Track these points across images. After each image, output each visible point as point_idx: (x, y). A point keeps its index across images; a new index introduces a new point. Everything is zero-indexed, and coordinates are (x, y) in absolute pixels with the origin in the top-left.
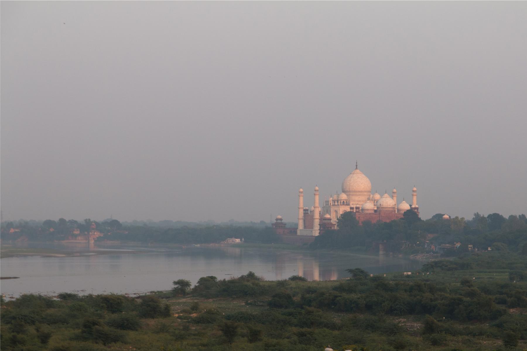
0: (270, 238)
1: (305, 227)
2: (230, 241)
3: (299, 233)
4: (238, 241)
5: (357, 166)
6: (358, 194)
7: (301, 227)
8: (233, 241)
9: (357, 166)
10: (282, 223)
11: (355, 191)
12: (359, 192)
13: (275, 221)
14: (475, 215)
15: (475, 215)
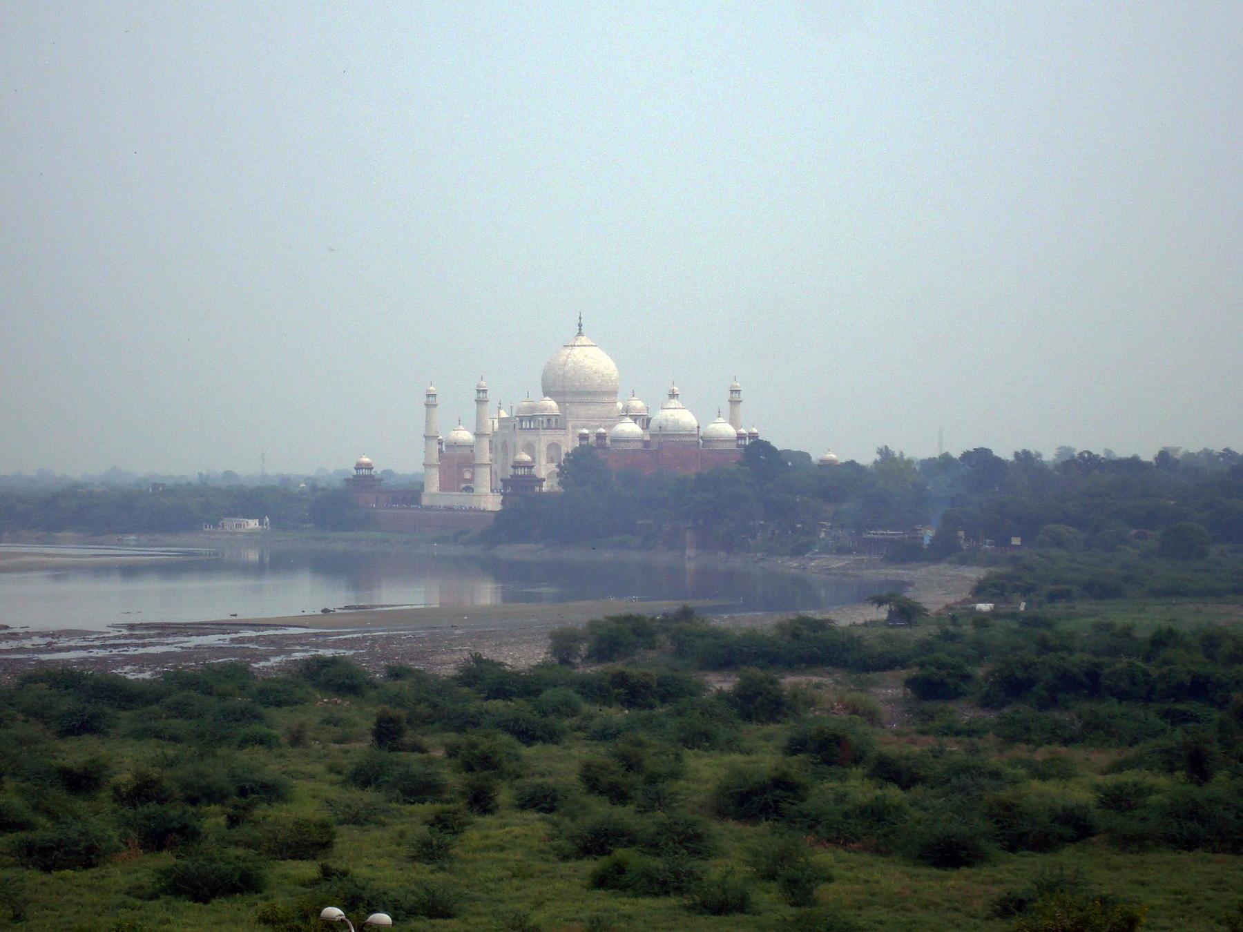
0: (339, 518)
1: (444, 486)
2: (230, 524)
3: (426, 501)
4: (253, 524)
5: (580, 325)
6: (586, 399)
7: (433, 485)
8: (239, 526)
9: (580, 325)
10: (371, 476)
11: (578, 393)
12: (590, 393)
13: (355, 472)
14: (880, 452)
15: (880, 452)
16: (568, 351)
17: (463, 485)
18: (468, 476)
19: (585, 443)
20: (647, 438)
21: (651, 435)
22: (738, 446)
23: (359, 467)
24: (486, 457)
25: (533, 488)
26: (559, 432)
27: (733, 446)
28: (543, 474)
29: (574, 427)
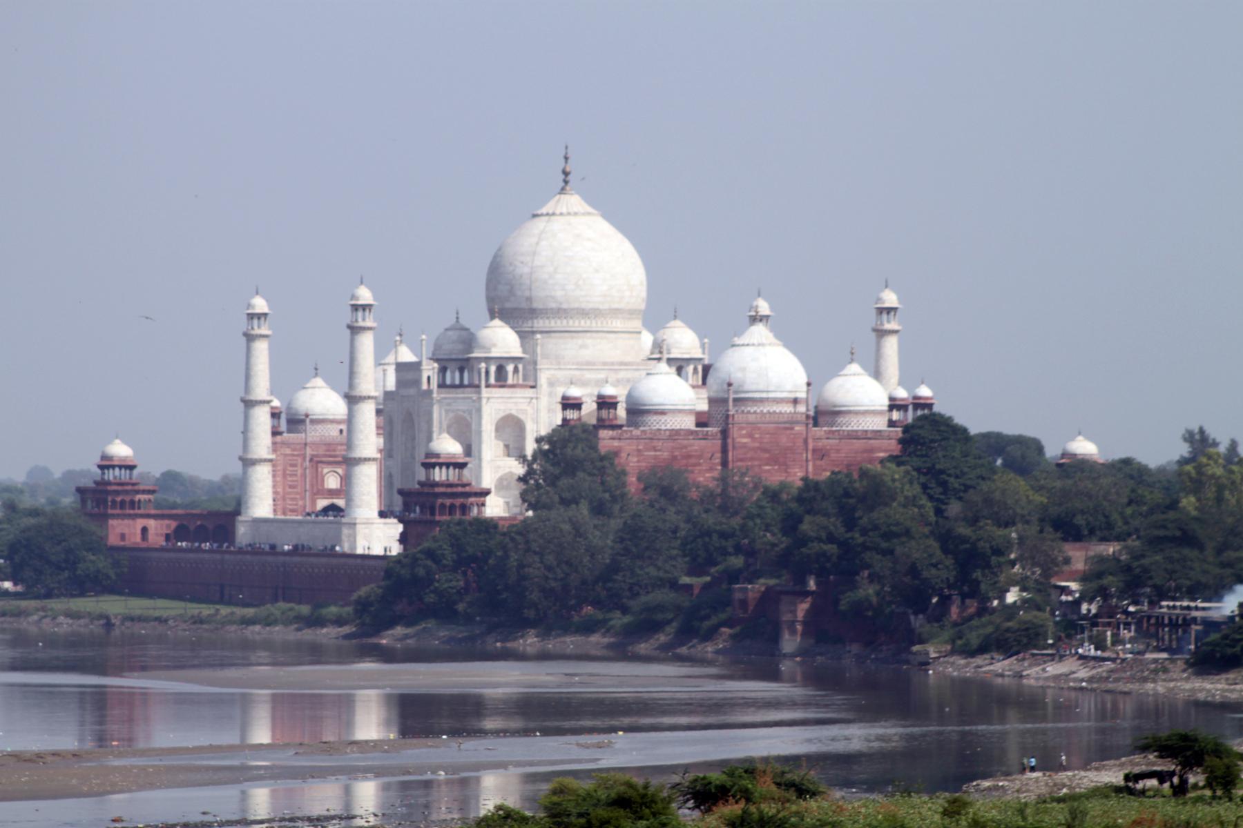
3: (243, 533)
9: (566, 173)
16: (540, 224)
17: (322, 503)
18: (332, 482)
19: (572, 415)
20: (703, 406)
21: (712, 401)
22: (892, 423)
23: (106, 464)
24: (369, 442)
25: (464, 509)
26: (520, 393)
27: (880, 424)
28: (487, 481)
29: (551, 384)
